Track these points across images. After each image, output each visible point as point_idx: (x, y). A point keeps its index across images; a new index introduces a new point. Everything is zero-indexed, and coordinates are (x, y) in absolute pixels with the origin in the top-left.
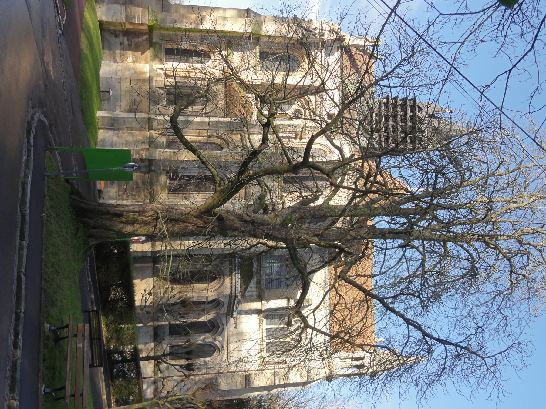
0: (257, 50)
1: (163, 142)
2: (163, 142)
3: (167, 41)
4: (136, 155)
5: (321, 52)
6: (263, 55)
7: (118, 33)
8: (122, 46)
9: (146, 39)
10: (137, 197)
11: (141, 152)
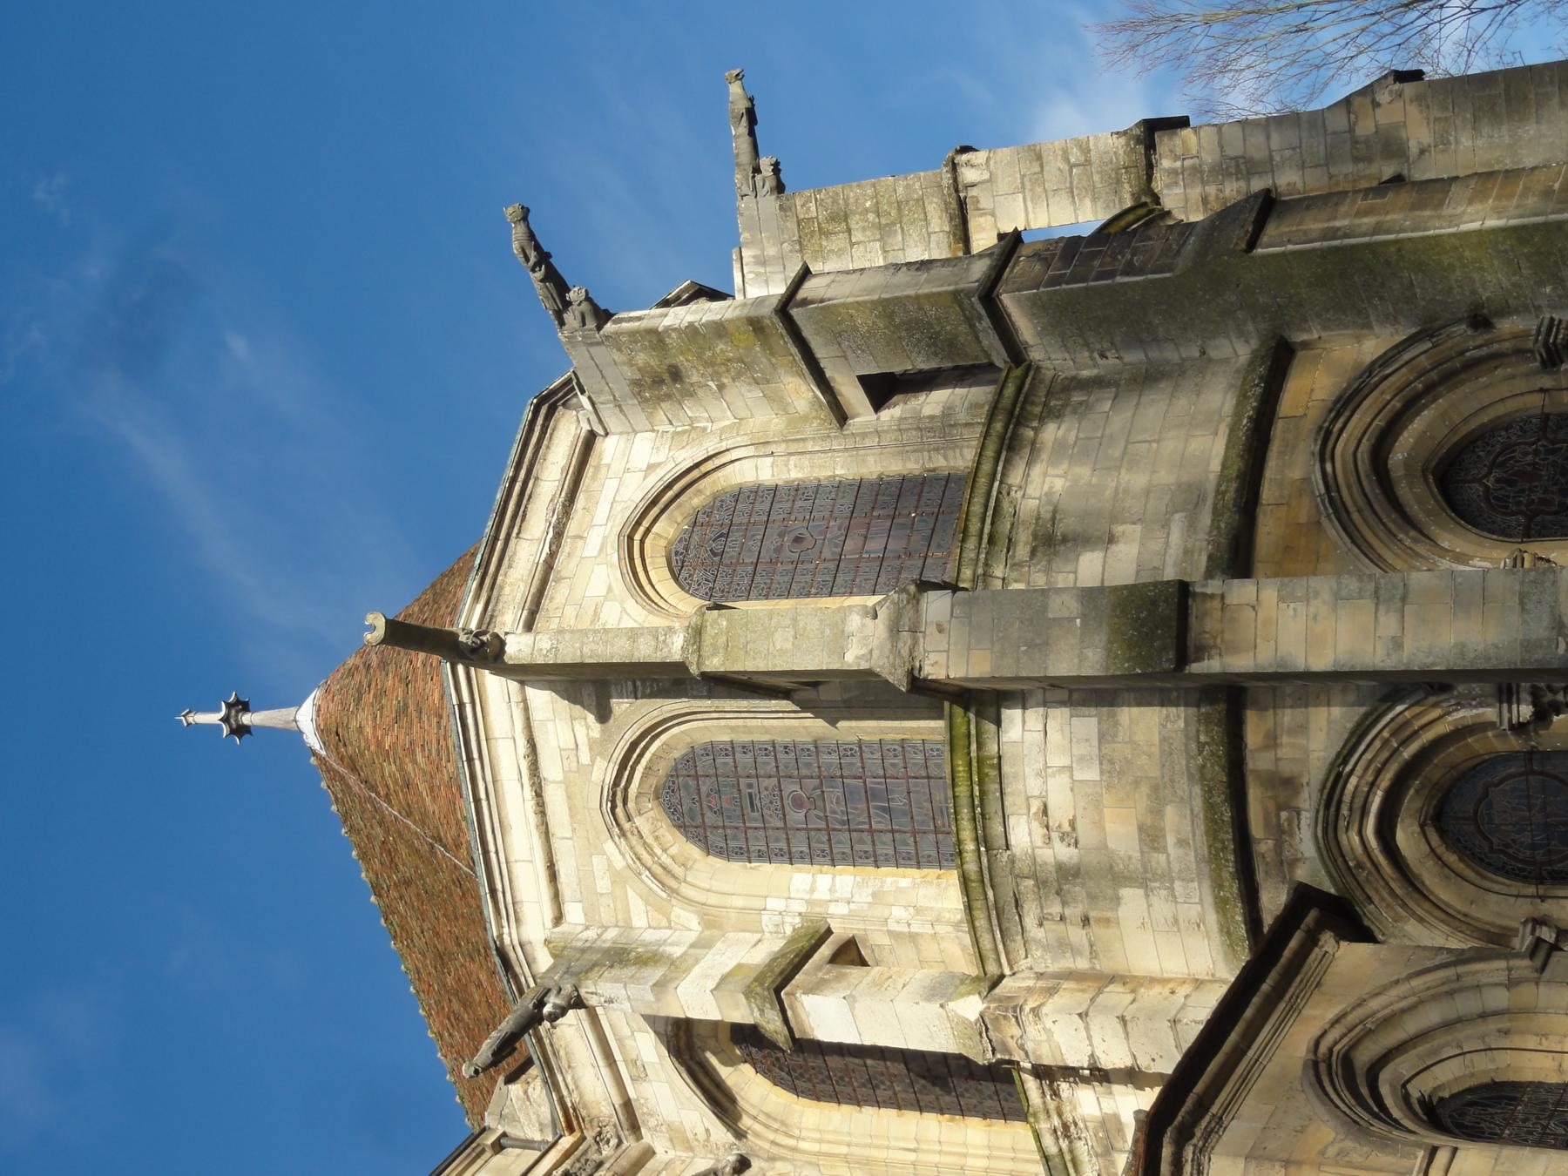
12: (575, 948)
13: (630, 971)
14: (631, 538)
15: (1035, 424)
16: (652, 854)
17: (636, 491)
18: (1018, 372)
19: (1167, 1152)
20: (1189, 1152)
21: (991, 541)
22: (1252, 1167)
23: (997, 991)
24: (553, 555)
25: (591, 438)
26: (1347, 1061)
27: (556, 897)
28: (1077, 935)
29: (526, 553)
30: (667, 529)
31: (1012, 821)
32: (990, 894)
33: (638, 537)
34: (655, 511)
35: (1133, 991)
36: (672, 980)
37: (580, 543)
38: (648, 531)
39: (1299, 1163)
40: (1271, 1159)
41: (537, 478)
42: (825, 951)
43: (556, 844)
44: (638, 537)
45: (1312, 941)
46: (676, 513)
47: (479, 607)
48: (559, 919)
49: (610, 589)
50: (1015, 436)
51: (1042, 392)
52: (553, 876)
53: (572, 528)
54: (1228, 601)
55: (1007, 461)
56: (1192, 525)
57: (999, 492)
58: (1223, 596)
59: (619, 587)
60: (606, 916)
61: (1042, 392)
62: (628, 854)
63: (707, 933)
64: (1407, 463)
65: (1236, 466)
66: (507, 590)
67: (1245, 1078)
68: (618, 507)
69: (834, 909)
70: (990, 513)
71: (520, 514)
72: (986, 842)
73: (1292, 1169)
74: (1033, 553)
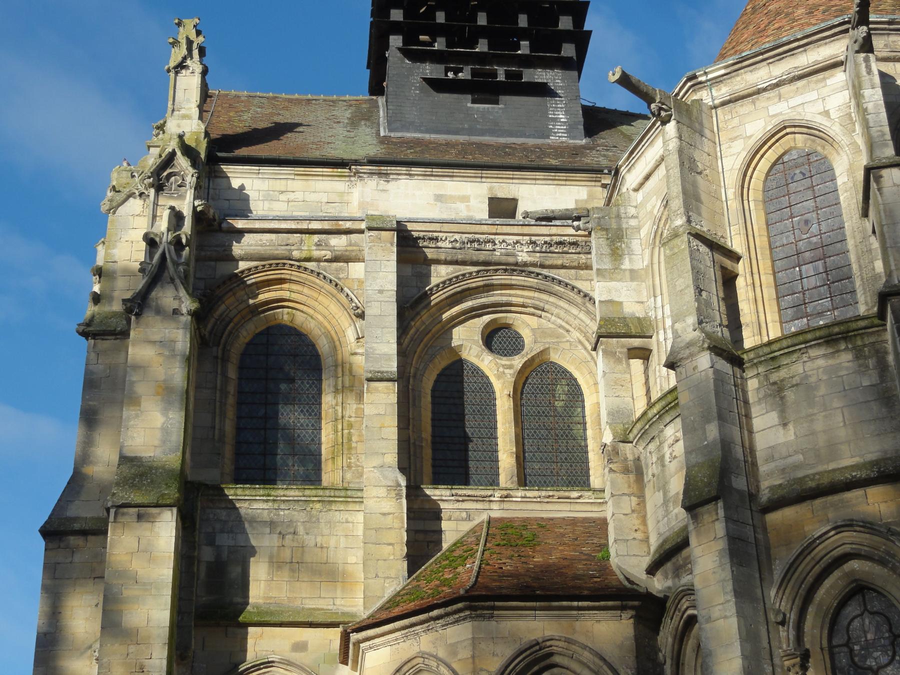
0: (232, 492)
5: (241, 232)
6: (261, 471)
12: (618, 211)
13: (606, 250)
14: (785, 128)
15: (850, 346)
16: (665, 225)
17: (811, 114)
18: (876, 321)
19: (460, 605)
20: (468, 613)
21: (773, 359)
22: (470, 642)
23: (621, 444)
24: (765, 90)
25: (841, 63)
26: (551, 654)
27: (642, 184)
28: (650, 473)
29: (762, 75)
30: (800, 140)
31: (672, 425)
32: (647, 427)
33: (788, 130)
34: (805, 130)
35: (633, 511)
36: (604, 276)
37: (777, 100)
38: (795, 133)
39: (474, 663)
40: (474, 648)
41: (805, 51)
42: (636, 342)
43: (656, 172)
44: (788, 130)
45: (623, 608)
46: (809, 142)
47: (723, 72)
48: (636, 190)
49: (751, 136)
50: (836, 341)
51: (872, 339)
52: (647, 178)
53: (784, 89)
54: (716, 523)
55: (819, 344)
57: (800, 349)
58: (718, 519)
59: (751, 142)
60: (641, 215)
61: (872, 339)
62: (660, 213)
63: (643, 272)
64: (853, 571)
65: (825, 481)
66: (738, 79)
67: (521, 616)
68: (800, 109)
69: (661, 332)
70: (786, 351)
71: (781, 57)
72: (660, 416)
73: (471, 660)
74: (775, 383)
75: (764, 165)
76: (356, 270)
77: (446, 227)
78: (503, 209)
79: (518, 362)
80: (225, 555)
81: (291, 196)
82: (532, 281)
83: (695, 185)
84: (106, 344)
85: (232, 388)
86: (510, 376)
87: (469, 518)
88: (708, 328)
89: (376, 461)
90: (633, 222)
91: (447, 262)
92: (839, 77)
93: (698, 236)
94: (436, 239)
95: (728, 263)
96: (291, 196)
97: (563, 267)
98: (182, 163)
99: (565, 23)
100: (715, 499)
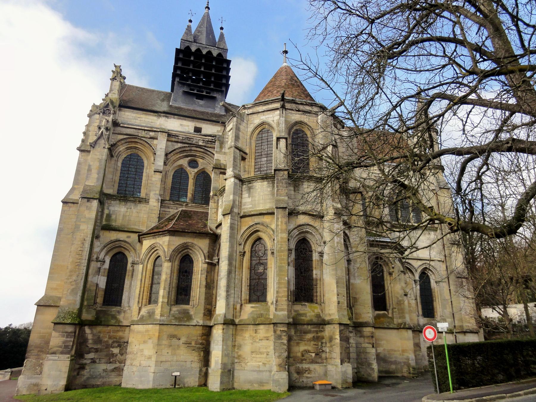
1: (252, 307)
2: (252, 307)
3: (95, 303)
4: (282, 339)
7: (78, 366)
8: (97, 361)
9: (91, 330)
10: (324, 341)
11: (278, 332)
13: (219, 146)
17: (270, 121)
42: (222, 171)
45: (207, 236)
53: (265, 113)
56: (250, 208)
59: (255, 125)
71: (265, 104)
75: (257, 131)
76: (155, 142)
77: (181, 133)
78: (198, 130)
79: (196, 170)
80: (111, 213)
81: (141, 119)
82: (202, 150)
83: (238, 134)
84: (83, 154)
85: (119, 169)
86: (193, 173)
87: (177, 209)
88: (235, 171)
89: (154, 192)
90: (227, 140)
91: (181, 143)
92: (278, 112)
93: (237, 148)
94: (178, 136)
95: (244, 155)
96: (141, 119)
97: (211, 147)
98: (111, 107)
99: (224, 81)
100: (229, 214)
